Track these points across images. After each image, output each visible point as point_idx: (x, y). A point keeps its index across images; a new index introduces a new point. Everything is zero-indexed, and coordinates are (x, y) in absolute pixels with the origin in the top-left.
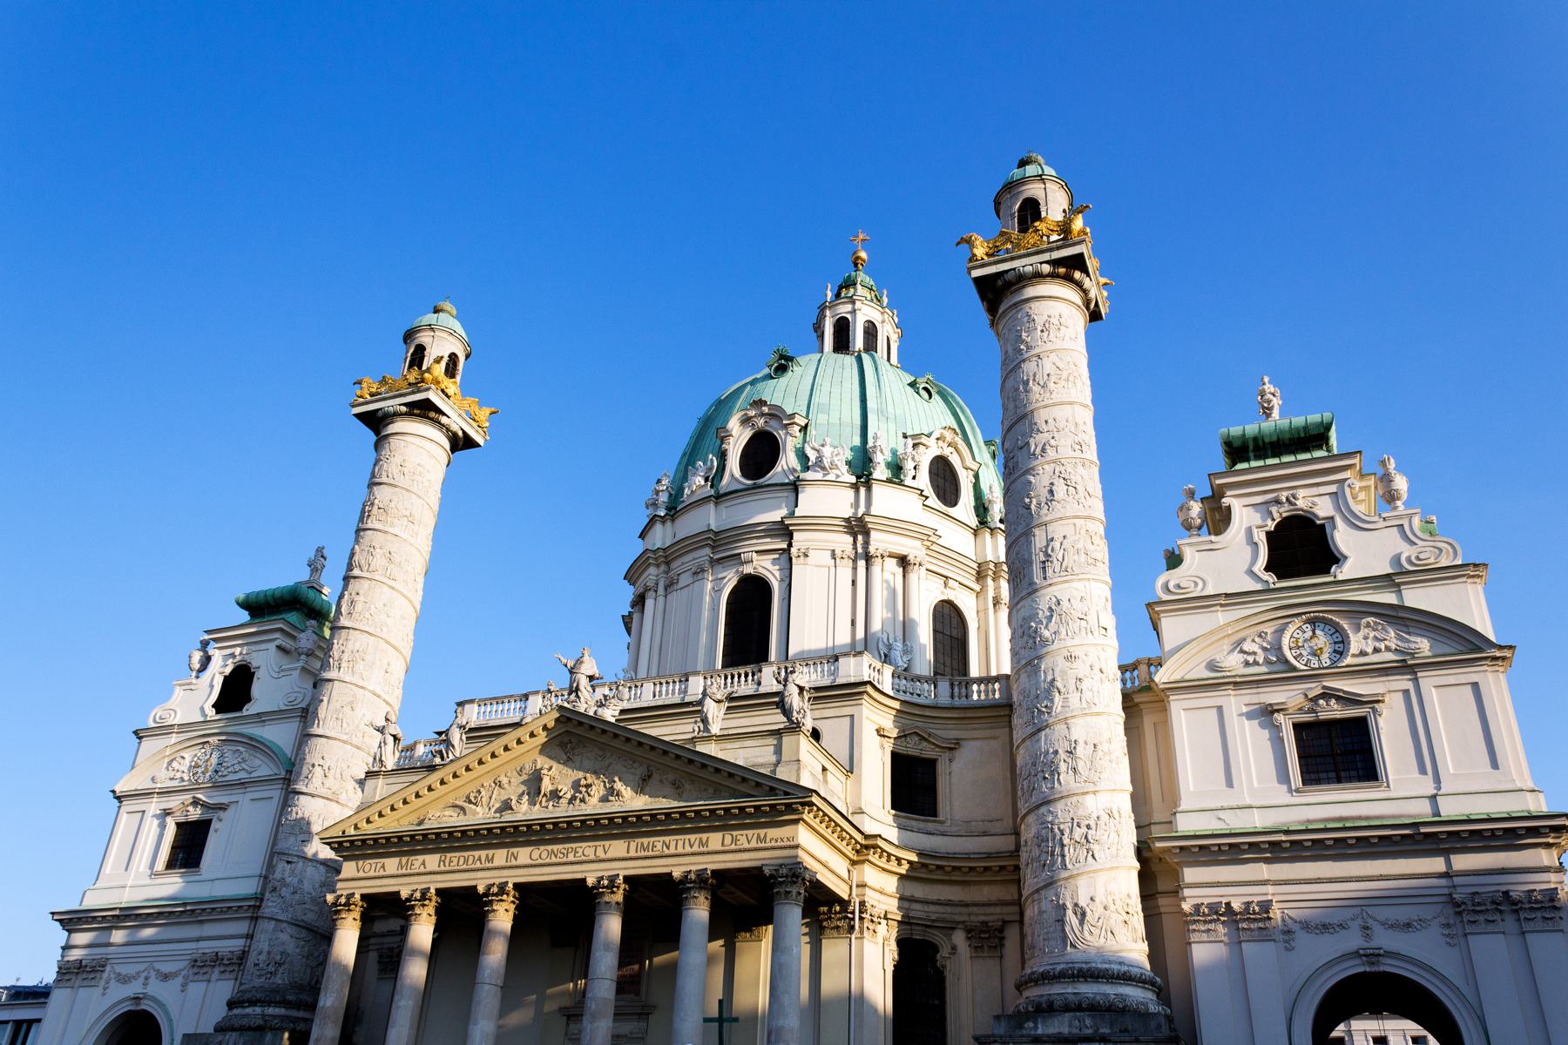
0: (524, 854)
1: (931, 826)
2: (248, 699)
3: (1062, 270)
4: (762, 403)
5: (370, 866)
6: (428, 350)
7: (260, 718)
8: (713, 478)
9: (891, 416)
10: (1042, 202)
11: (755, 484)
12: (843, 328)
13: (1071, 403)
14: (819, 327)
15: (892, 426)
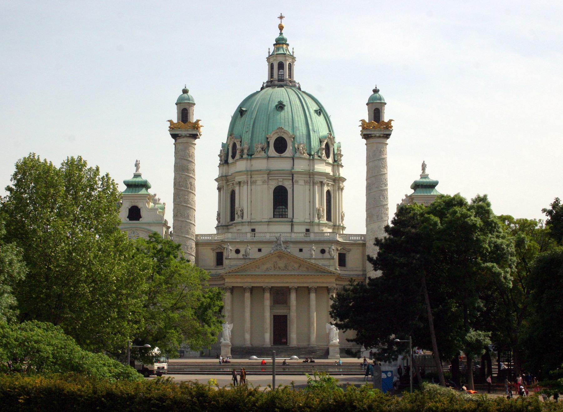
0: (273, 280)
1: (345, 269)
2: (141, 217)
3: (385, 136)
4: (282, 128)
5: (233, 280)
6: (188, 111)
7: (148, 224)
8: (265, 150)
9: (315, 130)
10: (380, 111)
11: (280, 156)
12: (281, 66)
13: (385, 174)
14: (269, 59)
15: (316, 134)
